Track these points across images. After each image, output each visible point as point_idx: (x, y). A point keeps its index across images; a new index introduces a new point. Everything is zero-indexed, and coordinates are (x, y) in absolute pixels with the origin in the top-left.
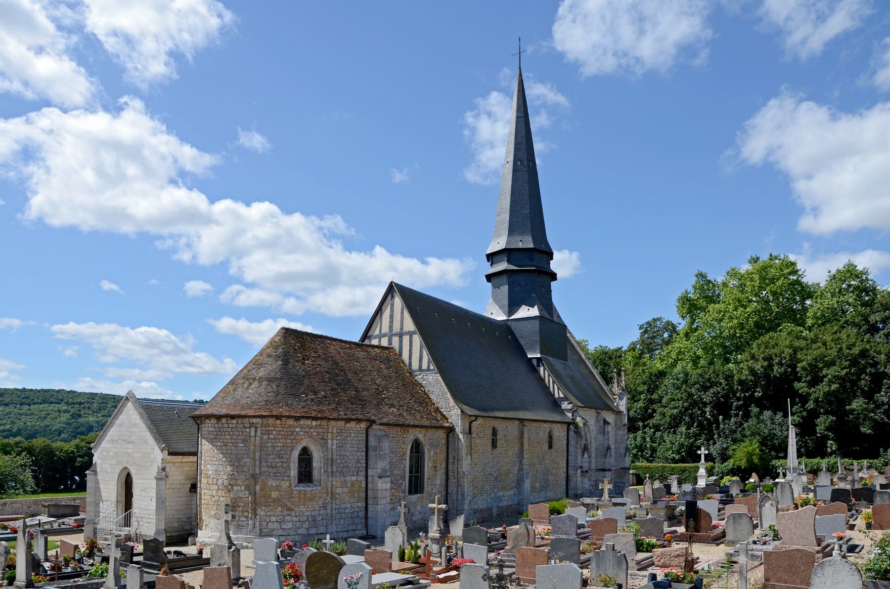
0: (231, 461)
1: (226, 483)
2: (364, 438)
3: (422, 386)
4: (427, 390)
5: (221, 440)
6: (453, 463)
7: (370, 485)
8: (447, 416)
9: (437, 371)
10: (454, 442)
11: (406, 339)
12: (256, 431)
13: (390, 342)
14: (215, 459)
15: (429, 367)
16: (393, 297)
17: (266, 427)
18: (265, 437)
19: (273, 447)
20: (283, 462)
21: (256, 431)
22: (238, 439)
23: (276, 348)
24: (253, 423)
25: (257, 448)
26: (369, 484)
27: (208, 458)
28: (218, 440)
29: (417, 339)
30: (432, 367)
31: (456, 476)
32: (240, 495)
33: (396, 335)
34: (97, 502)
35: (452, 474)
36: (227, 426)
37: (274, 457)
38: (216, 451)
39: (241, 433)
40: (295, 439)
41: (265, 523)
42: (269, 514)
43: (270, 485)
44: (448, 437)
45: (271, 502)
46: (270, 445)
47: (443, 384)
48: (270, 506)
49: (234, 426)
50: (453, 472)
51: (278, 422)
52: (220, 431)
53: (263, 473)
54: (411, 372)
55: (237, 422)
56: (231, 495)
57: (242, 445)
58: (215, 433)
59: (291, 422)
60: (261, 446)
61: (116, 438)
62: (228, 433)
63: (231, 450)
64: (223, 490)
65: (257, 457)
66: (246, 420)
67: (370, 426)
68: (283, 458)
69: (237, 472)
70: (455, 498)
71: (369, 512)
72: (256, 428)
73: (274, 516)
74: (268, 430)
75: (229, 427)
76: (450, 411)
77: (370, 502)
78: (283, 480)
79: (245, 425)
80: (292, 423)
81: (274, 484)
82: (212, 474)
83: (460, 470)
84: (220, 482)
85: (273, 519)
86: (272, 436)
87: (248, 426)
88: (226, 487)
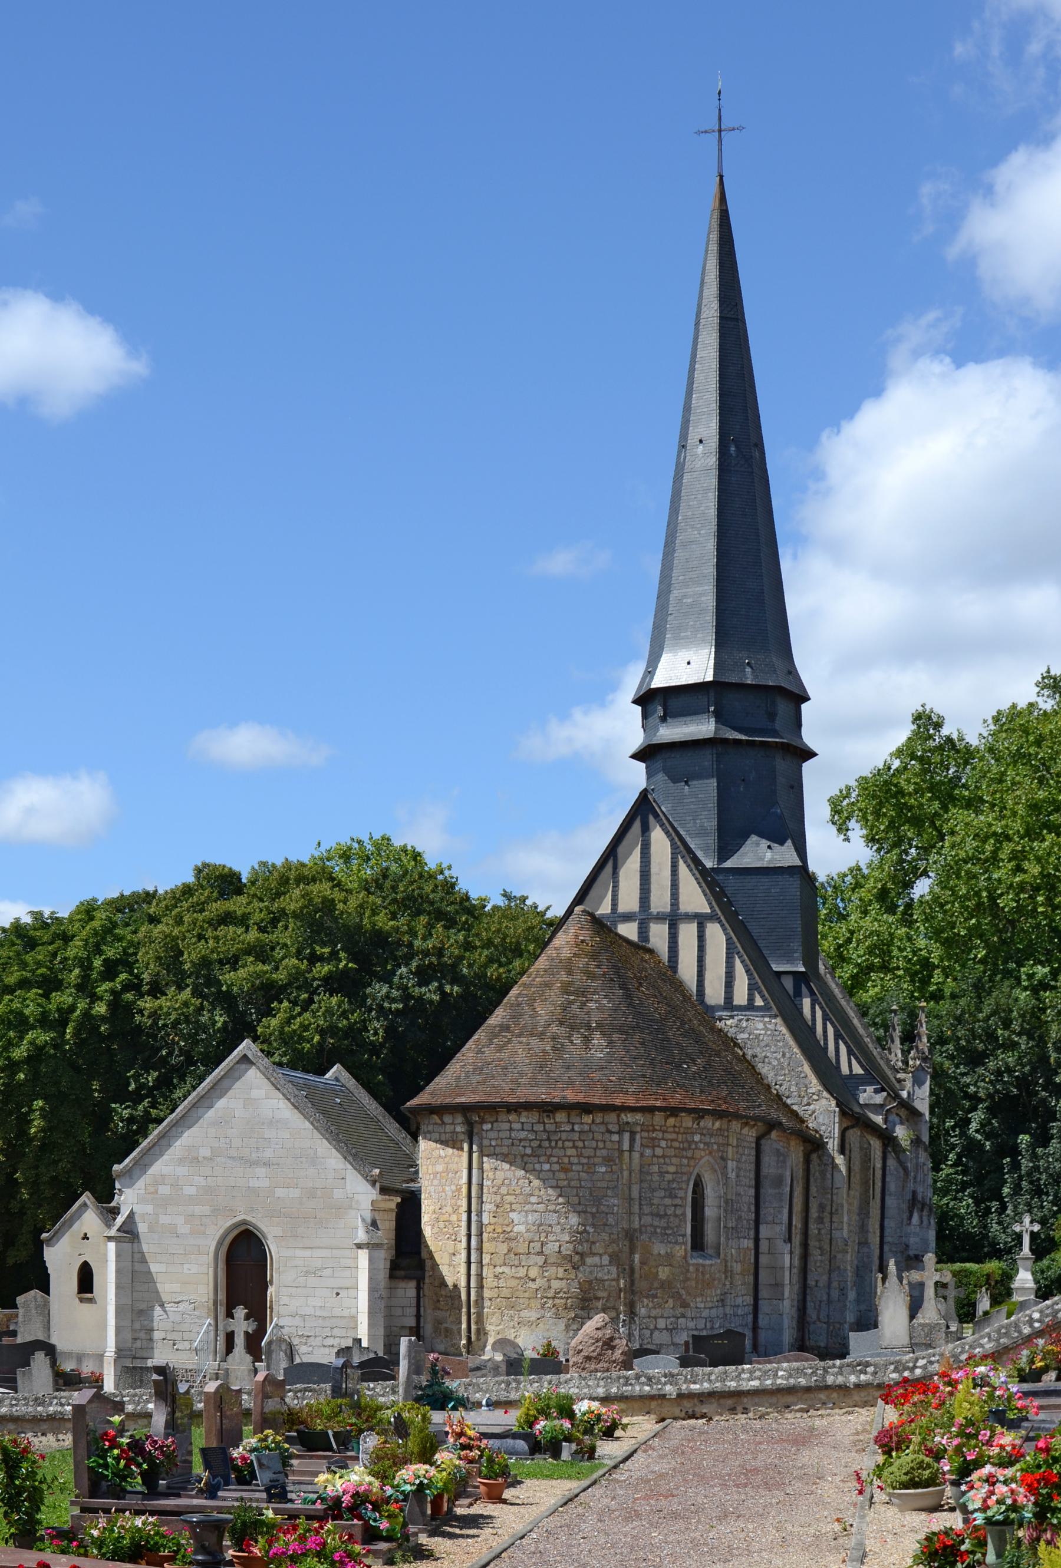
0: (579, 1204)
1: (567, 1250)
2: (753, 1159)
3: (736, 1045)
4: (749, 1053)
5: (555, 1160)
6: (820, 1220)
7: (763, 1260)
8: (801, 1113)
9: (775, 1011)
10: (823, 1173)
11: (688, 933)
12: (632, 1140)
13: (643, 932)
14: (533, 1199)
15: (751, 999)
16: (646, 829)
17: (648, 1131)
18: (648, 1152)
19: (662, 1174)
20: (676, 1206)
21: (632, 1140)
22: (595, 1156)
23: (594, 956)
24: (628, 1123)
25: (635, 1177)
26: (761, 1256)
27: (510, 1199)
28: (542, 1159)
29: (717, 936)
30: (759, 1002)
31: (827, 1247)
32: (600, 1275)
33: (660, 918)
34: (143, 1306)
35: (817, 1244)
36: (568, 1128)
37: (663, 1194)
38: (536, 1183)
39: (601, 1145)
40: (692, 1158)
41: (647, 1333)
42: (654, 1313)
43: (656, 1252)
44: (807, 1161)
45: (657, 1289)
46: (655, 1168)
47: (792, 1043)
48: (655, 1296)
49: (586, 1128)
50: (820, 1240)
51: (671, 1121)
52: (549, 1139)
53: (643, 1229)
54: (708, 1012)
55: (593, 1121)
56: (580, 1275)
57: (603, 1169)
58: (535, 1144)
59: (688, 1121)
60: (641, 1171)
61: (205, 1152)
62: (570, 1144)
63: (580, 1180)
64: (559, 1265)
65: (635, 1194)
66: (612, 1117)
67: (768, 1132)
68: (676, 1197)
69: (593, 1225)
70: (825, 1298)
71: (761, 1316)
72: (633, 1134)
73: (662, 1317)
74: (653, 1139)
75: (573, 1130)
76: (809, 1104)
77: (763, 1293)
78: (676, 1243)
79: (610, 1127)
80: (690, 1124)
81: (662, 1252)
82: (528, 1231)
83: (836, 1234)
84: (552, 1248)
85: (661, 1323)
86: (659, 1152)
87: (615, 1128)
88: (568, 1258)
